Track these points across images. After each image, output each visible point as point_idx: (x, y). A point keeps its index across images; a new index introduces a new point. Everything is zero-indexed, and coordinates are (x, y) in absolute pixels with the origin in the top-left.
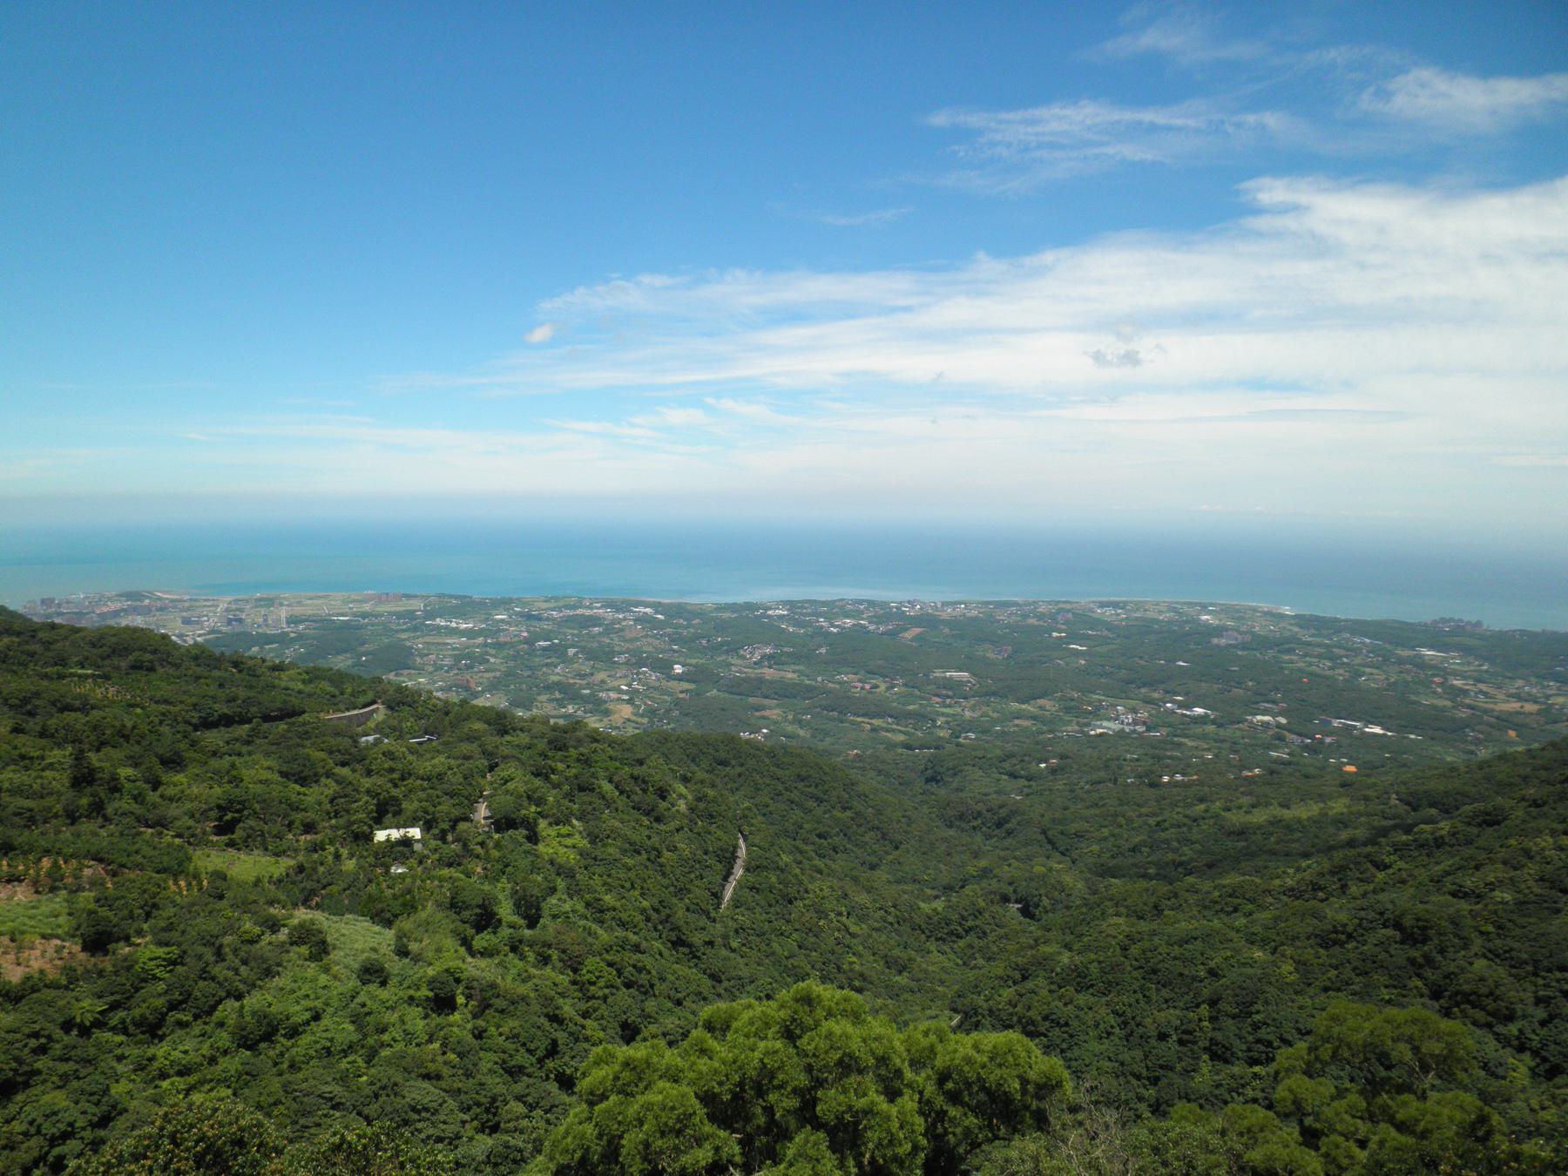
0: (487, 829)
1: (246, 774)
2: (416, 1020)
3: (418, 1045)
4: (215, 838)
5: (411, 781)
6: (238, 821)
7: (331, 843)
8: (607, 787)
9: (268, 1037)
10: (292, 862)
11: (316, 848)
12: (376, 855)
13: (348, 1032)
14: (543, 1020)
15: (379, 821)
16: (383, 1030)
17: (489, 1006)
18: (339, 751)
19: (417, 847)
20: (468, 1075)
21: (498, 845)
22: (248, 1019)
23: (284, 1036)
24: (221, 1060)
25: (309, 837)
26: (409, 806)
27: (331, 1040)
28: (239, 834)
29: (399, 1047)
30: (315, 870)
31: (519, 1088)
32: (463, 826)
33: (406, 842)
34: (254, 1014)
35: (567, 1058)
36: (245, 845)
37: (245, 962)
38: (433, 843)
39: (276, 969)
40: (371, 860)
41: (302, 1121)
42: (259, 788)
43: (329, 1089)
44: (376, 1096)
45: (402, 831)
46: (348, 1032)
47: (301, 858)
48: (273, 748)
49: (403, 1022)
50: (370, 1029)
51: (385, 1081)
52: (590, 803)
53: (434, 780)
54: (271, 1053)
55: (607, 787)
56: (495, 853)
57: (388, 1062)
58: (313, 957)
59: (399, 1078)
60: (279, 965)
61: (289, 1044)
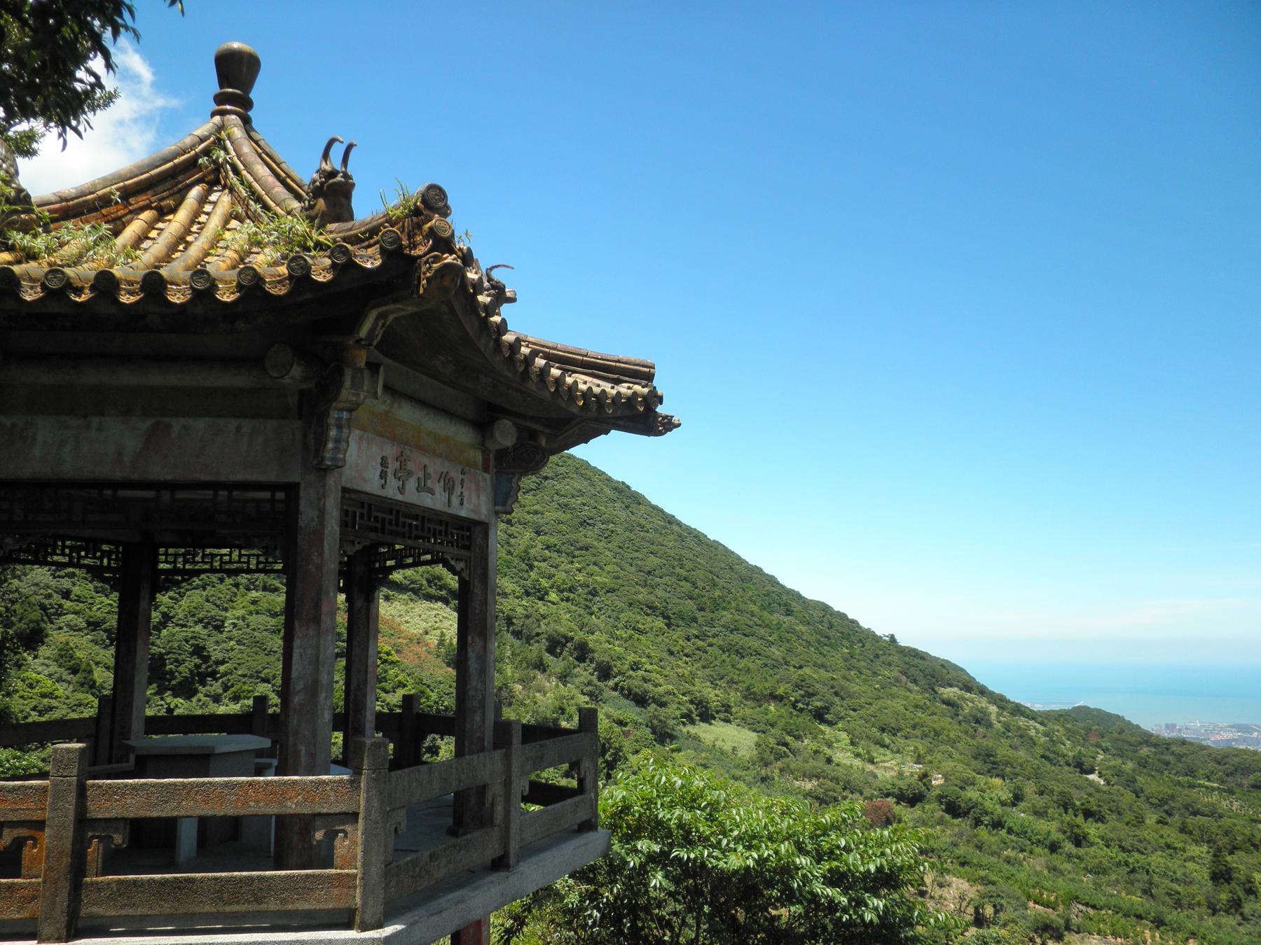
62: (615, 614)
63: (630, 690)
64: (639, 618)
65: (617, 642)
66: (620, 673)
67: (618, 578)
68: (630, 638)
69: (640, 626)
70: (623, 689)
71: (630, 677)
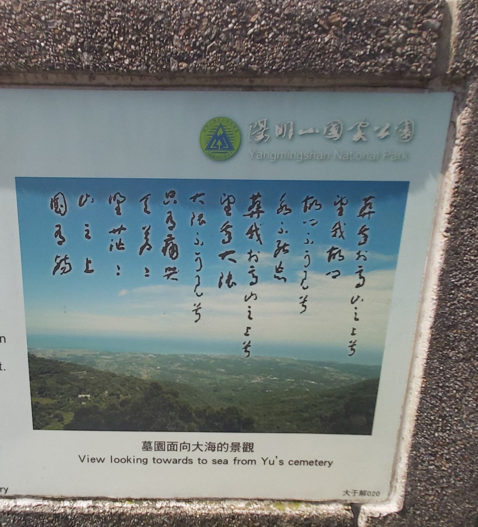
8: (137, 388)
19: (89, 399)
21: (109, 399)
26: (88, 390)
28: (44, 394)
32: (100, 395)
36: (46, 396)
55: (137, 388)
56: (108, 401)
58: (59, 421)
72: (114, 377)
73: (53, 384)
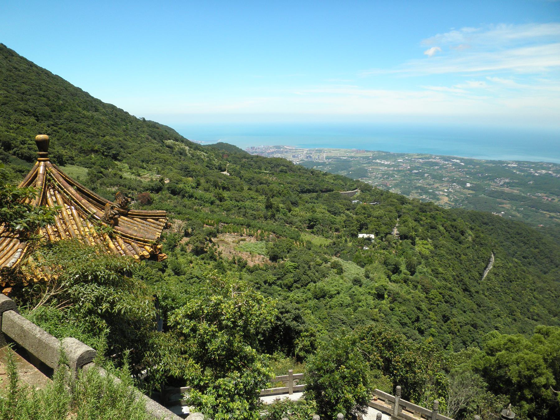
0: (397, 238)
1: (318, 210)
2: (371, 300)
3: (371, 309)
4: (308, 230)
5: (371, 218)
6: (315, 225)
7: (344, 236)
9: (323, 297)
10: (332, 241)
11: (339, 237)
12: (359, 242)
13: (348, 300)
14: (415, 308)
15: (360, 230)
16: (360, 302)
17: (396, 300)
18: (346, 205)
19: (373, 241)
20: (388, 322)
21: (401, 244)
22: (318, 290)
23: (328, 297)
24: (308, 301)
25: (337, 233)
26: (371, 227)
27: (343, 301)
28: (315, 229)
29: (365, 308)
30: (339, 244)
31: (405, 330)
32: (389, 236)
33: (369, 239)
34: (319, 288)
35: (422, 323)
37: (317, 272)
38: (378, 241)
39: (326, 275)
40: (357, 243)
41: (333, 326)
42: (321, 215)
43: (342, 317)
44: (357, 323)
45: (368, 235)
46: (348, 300)
47: (334, 240)
48: (325, 202)
49: (366, 300)
50: (356, 300)
51: (360, 318)
52: (435, 233)
53: (379, 219)
54: (324, 302)
55: (442, 228)
56: (400, 247)
57: (361, 312)
58: (338, 273)
59: (365, 319)
60: (327, 274)
61: (330, 300)
62: (7, 116)
63: (22, 154)
64: (21, 117)
65: (11, 131)
66: (16, 147)
67: (7, 97)
68: (18, 128)
69: (22, 121)
70: (18, 154)
71: (22, 148)
72: (403, 204)
73: (323, 213)
